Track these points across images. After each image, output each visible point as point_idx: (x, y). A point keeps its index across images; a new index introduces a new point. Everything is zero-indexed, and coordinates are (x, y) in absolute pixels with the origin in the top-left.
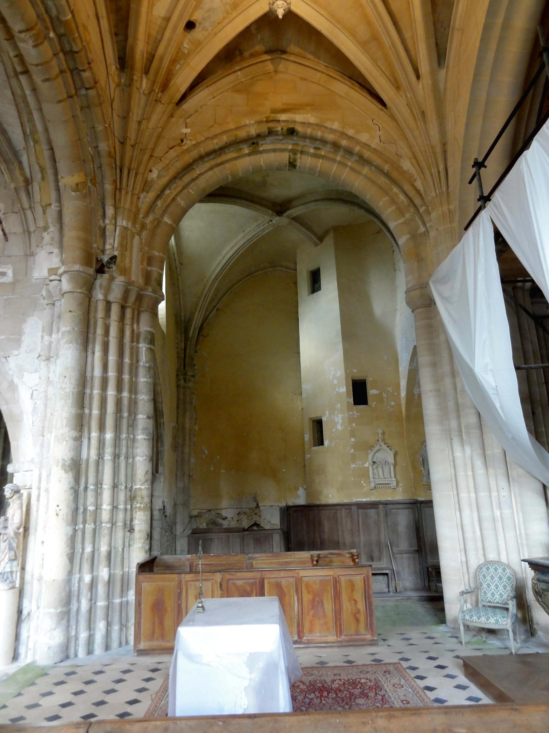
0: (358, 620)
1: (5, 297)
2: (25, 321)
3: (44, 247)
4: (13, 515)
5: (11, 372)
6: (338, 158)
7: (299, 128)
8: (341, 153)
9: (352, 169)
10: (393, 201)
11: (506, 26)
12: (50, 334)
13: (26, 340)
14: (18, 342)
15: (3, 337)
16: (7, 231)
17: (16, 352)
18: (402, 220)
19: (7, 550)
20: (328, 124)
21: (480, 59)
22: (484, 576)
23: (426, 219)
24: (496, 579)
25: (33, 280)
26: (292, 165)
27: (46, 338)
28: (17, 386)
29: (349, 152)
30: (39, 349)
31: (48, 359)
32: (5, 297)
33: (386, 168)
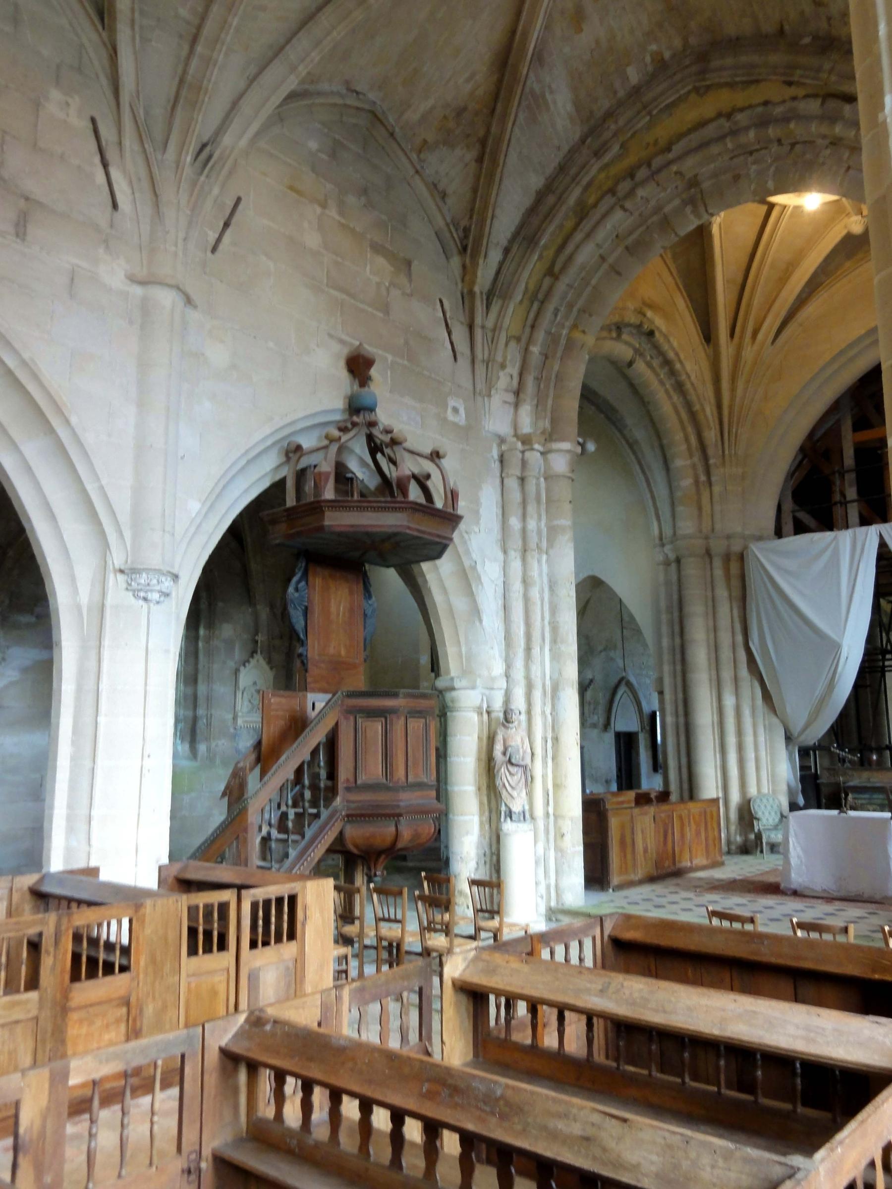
0: (715, 845)
6: (662, 376)
7: (657, 334)
8: (666, 369)
9: (667, 391)
10: (687, 439)
11: (852, 360)
18: (689, 462)
20: (671, 339)
21: (823, 369)
22: (759, 806)
23: (713, 471)
24: (769, 808)
26: (630, 364)
29: (673, 373)
33: (697, 407)
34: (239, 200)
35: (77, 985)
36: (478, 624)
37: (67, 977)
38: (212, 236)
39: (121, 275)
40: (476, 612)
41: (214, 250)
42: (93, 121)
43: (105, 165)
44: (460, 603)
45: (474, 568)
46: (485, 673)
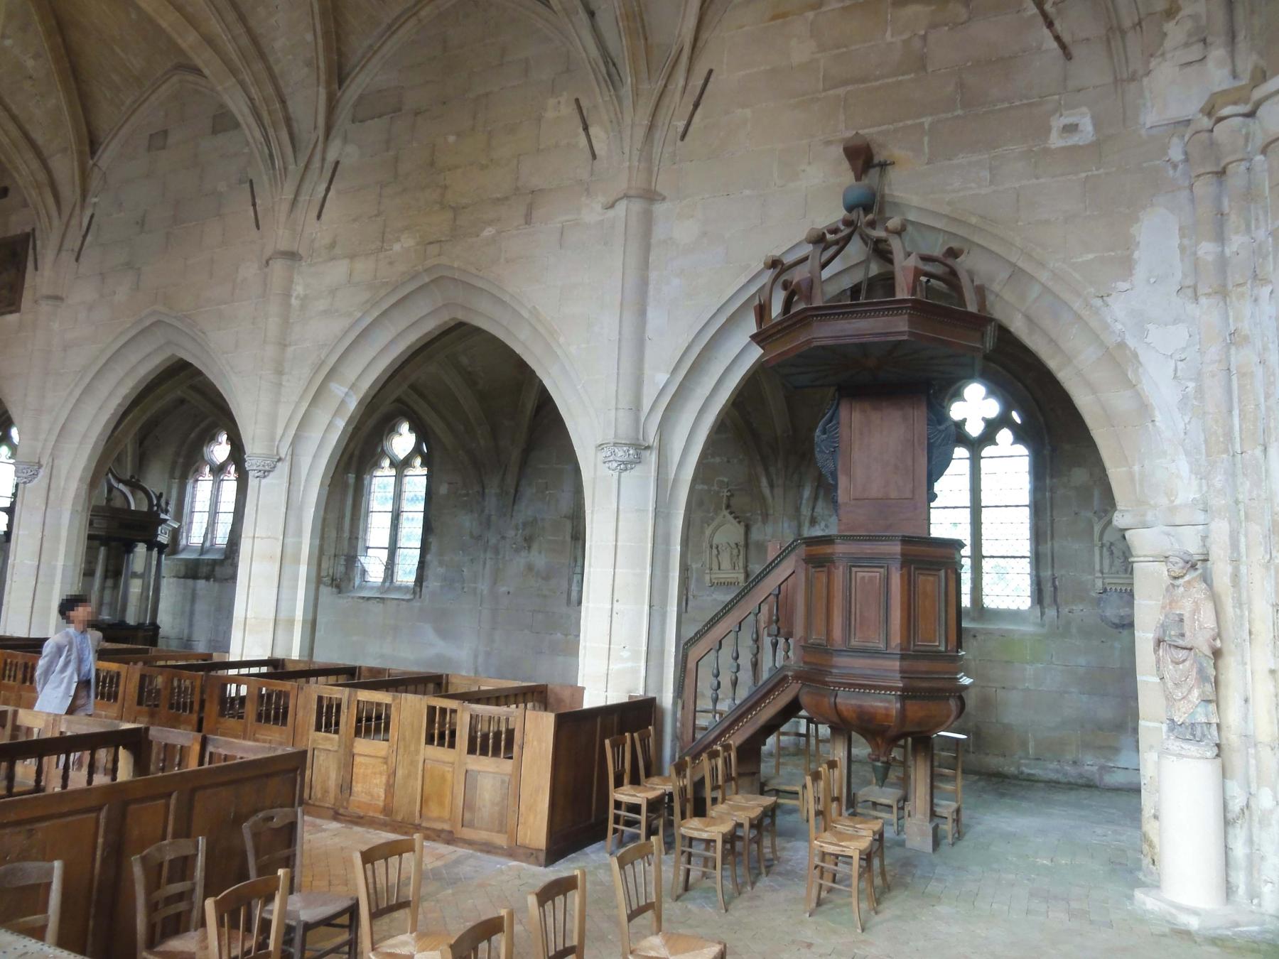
1: (1083, 175)
2: (1137, 220)
3: (1168, 56)
4: (1196, 610)
5: (1119, 326)
12: (1220, 237)
13: (1144, 258)
14: (1126, 266)
15: (1091, 256)
16: (1067, 38)
17: (1123, 285)
19: (1191, 681)
25: (1143, 132)
27: (1207, 249)
28: (1136, 356)
30: (1179, 275)
31: (1222, 292)
32: (1083, 175)
34: (711, 72)
35: (358, 739)
36: (1150, 425)
37: (353, 731)
38: (681, 125)
39: (598, 208)
40: (1144, 409)
41: (683, 137)
42: (577, 100)
43: (586, 129)
44: (1120, 401)
45: (1122, 345)
46: (1163, 501)
